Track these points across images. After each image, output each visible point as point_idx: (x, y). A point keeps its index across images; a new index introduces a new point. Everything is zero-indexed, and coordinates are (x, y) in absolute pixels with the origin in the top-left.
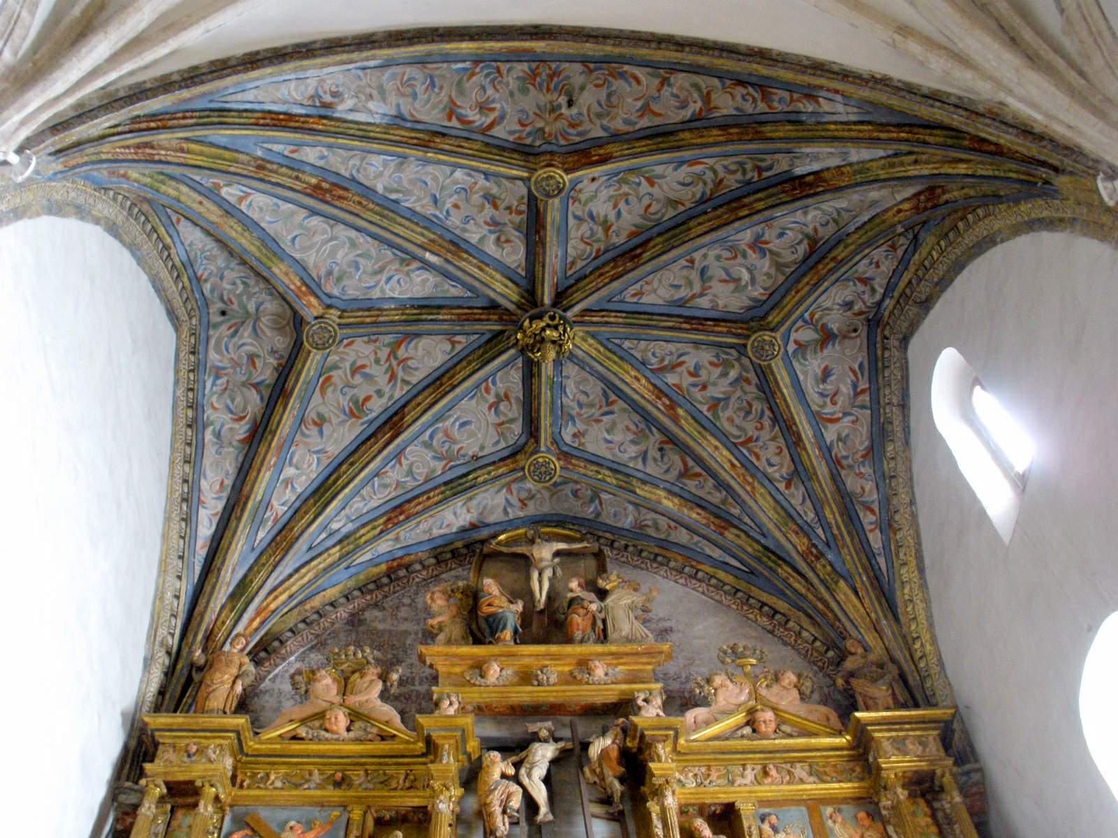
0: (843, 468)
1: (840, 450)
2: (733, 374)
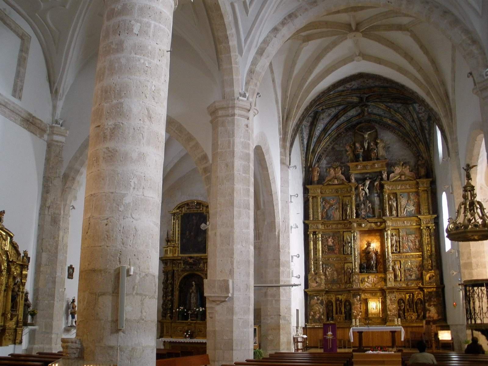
1: (422, 118)
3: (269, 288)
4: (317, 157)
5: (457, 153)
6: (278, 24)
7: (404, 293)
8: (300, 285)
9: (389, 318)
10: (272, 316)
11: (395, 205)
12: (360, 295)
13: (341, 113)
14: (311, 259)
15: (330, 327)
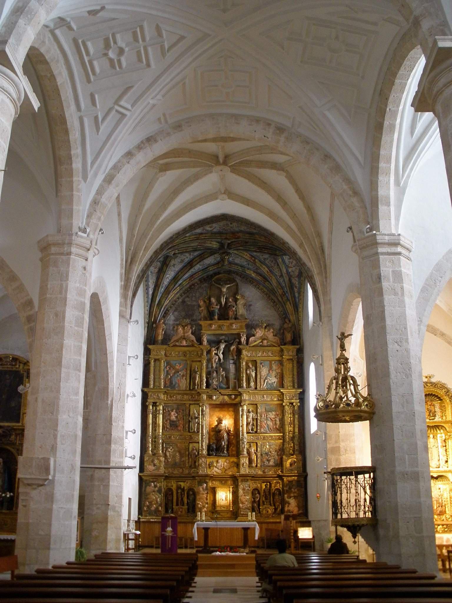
1: (292, 273)
3: (97, 471)
4: (163, 310)
5: (330, 318)
6: (133, 148)
7: (260, 482)
8: (135, 467)
9: (241, 511)
10: (98, 506)
11: (254, 375)
12: (206, 483)
13: (196, 261)
14: (149, 436)
15: (170, 521)
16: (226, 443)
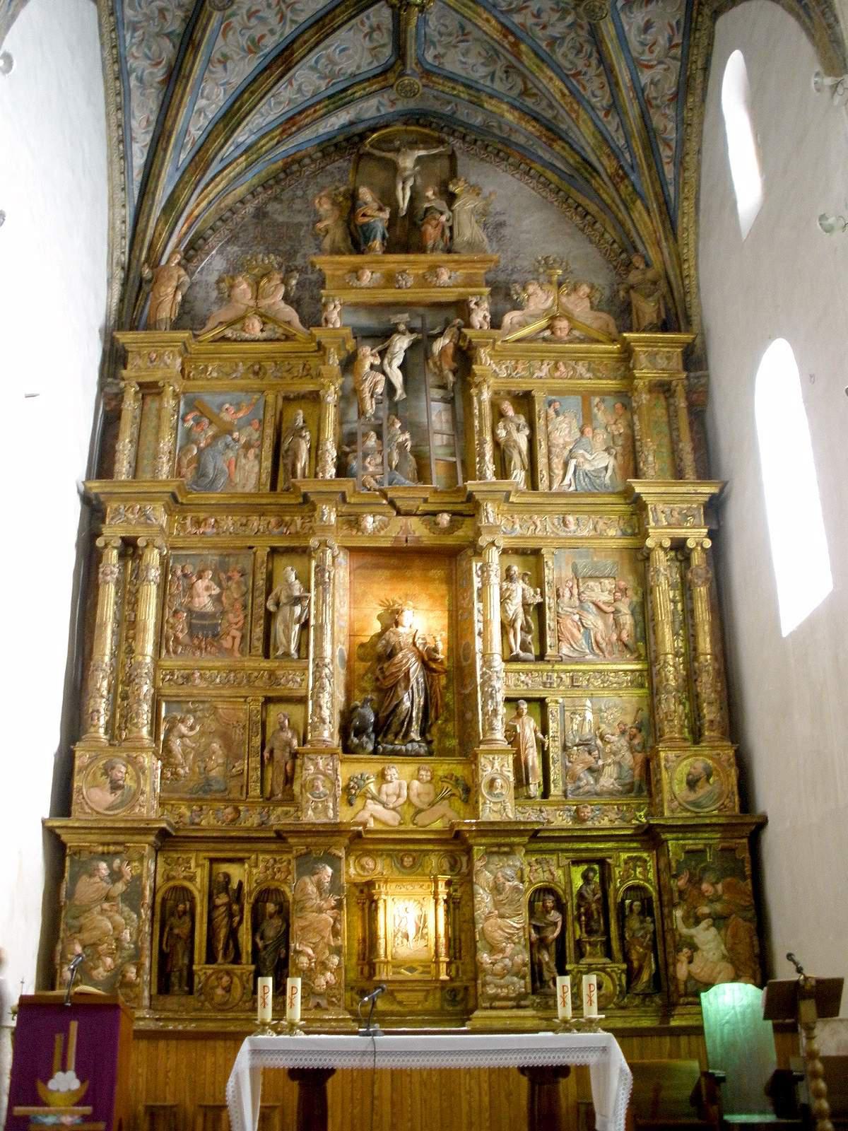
0: (652, 106)
1: (651, 92)
2: (570, 19)
7: (565, 862)
9: (485, 984)
11: (523, 444)
16: (420, 700)
